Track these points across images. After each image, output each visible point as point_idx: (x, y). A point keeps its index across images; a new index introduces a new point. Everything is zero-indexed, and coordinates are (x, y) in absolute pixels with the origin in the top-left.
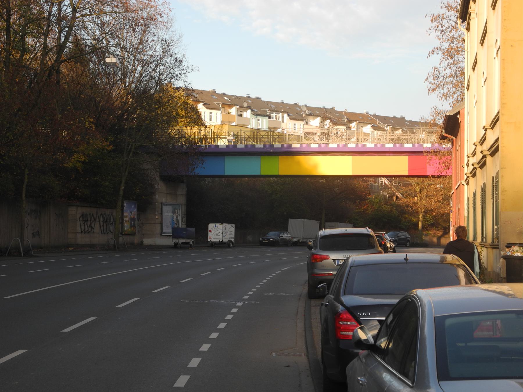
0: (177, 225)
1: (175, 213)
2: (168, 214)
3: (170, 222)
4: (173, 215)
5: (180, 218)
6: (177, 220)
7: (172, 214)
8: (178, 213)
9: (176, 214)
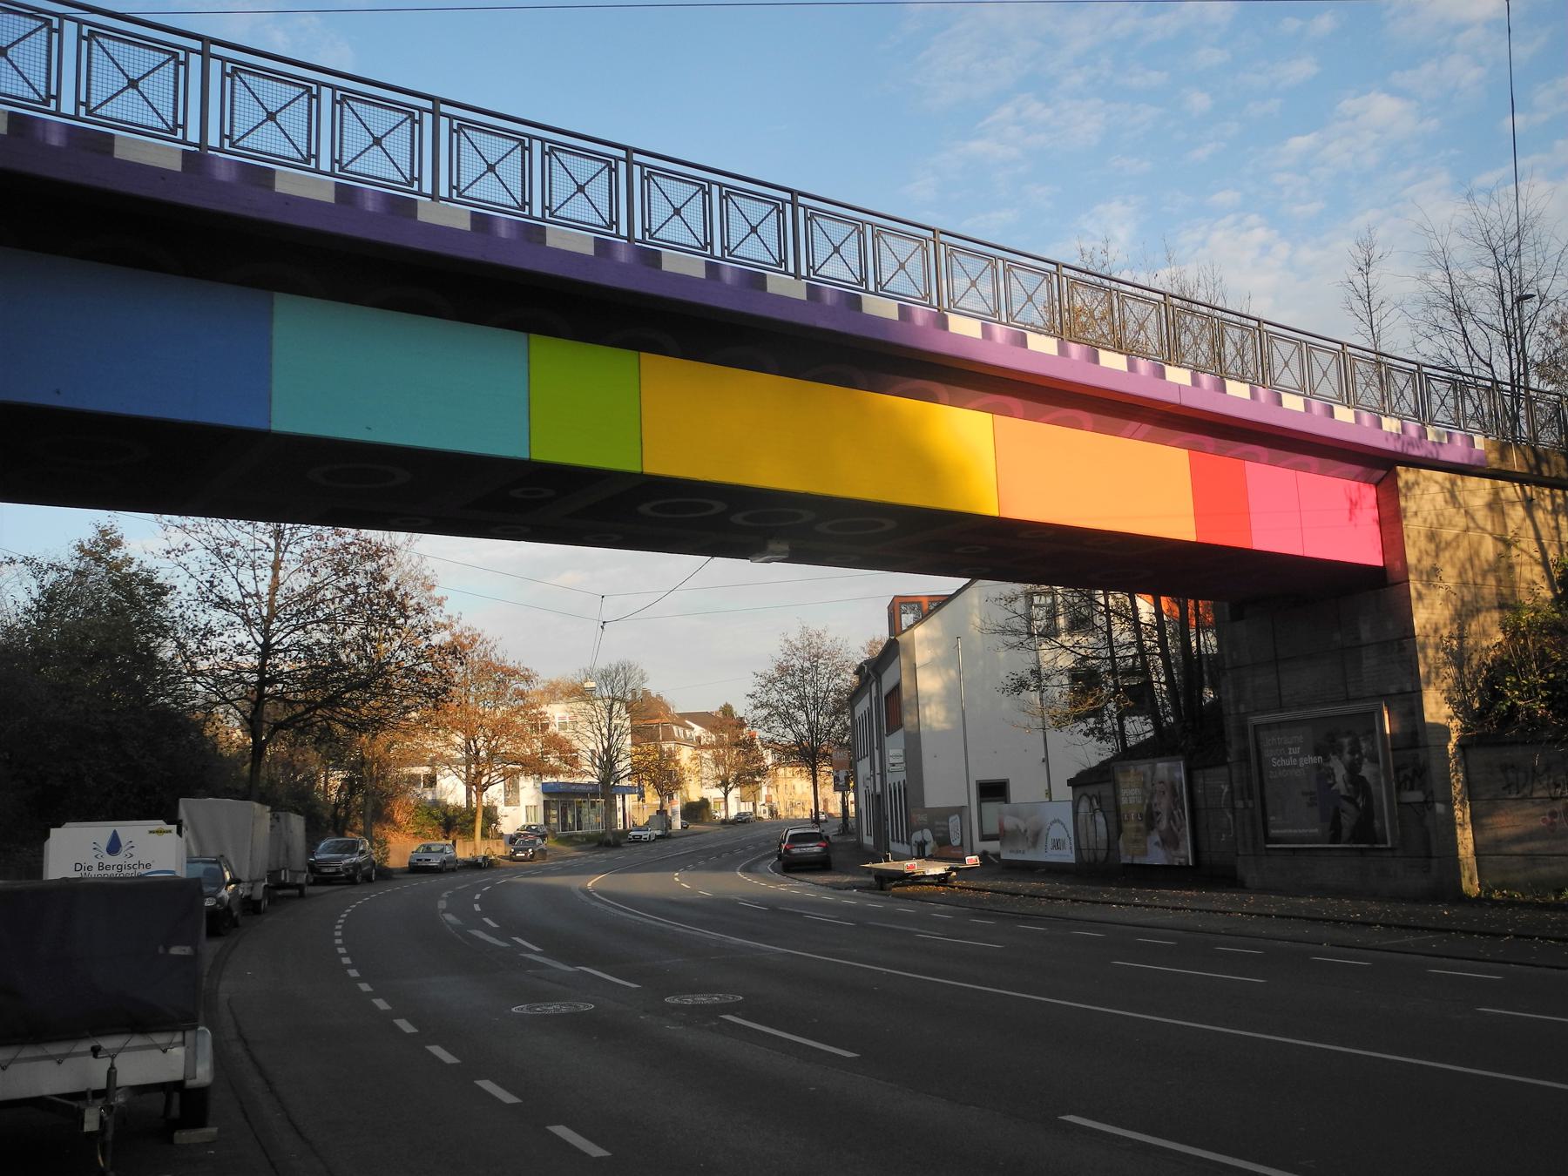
0: (1357, 806)
1: (1338, 751)
2: (1293, 762)
4: (1327, 759)
7: (1312, 760)
8: (1355, 749)
9: (1347, 757)
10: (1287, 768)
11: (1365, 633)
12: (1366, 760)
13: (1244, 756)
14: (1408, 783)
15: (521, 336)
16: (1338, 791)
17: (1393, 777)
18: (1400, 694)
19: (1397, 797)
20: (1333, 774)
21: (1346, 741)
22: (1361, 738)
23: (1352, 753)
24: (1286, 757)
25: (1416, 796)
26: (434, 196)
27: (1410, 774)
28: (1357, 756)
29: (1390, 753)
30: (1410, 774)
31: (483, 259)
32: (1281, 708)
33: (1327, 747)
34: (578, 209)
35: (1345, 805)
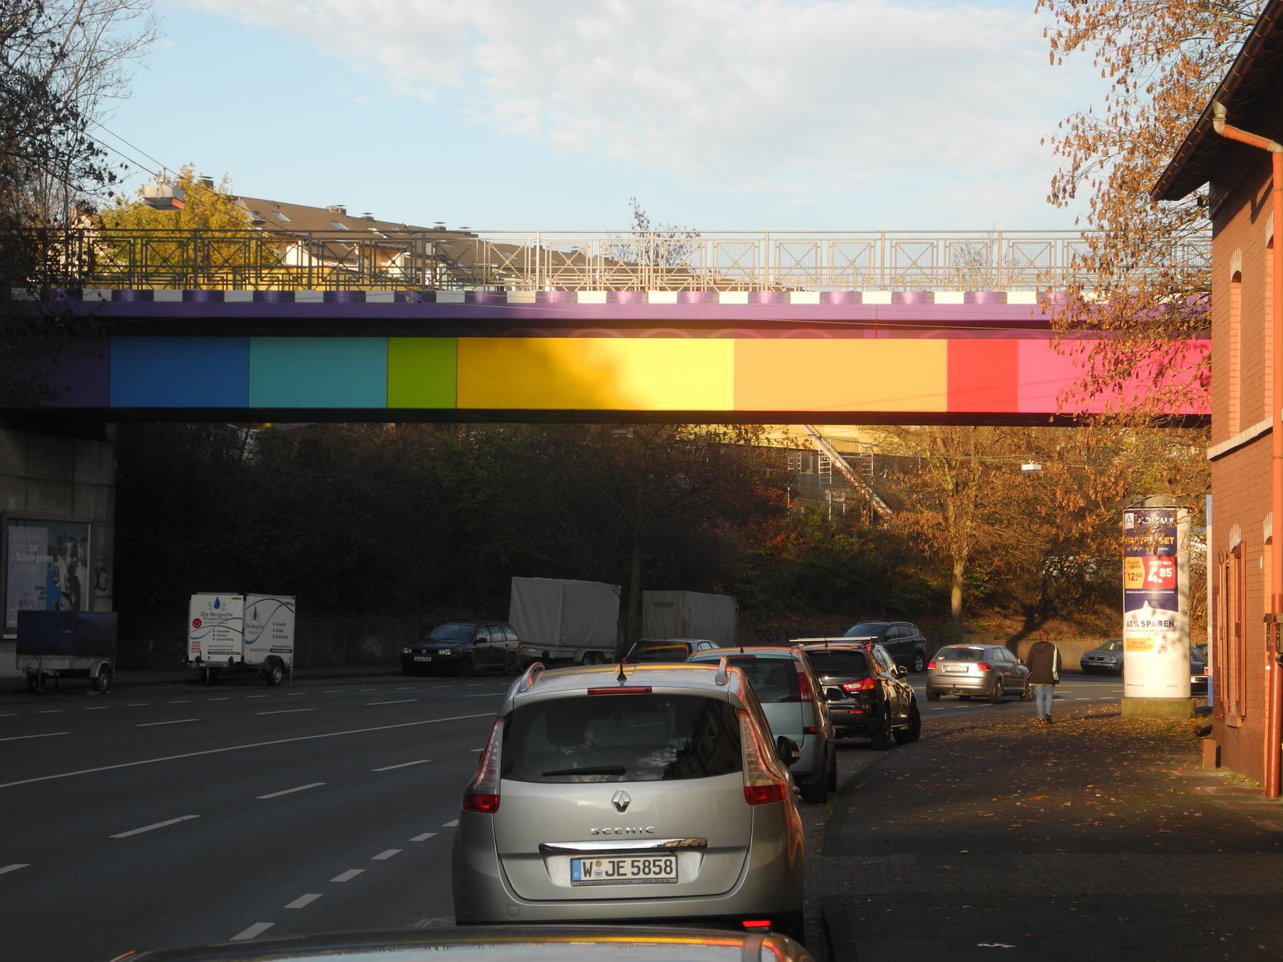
0: (70, 601)
1: (64, 553)
2: (31, 558)
3: (42, 588)
4: (56, 560)
5: (83, 574)
6: (73, 580)
7: (47, 558)
8: (74, 554)
9: (69, 558)
12: (80, 563)
21: (69, 545)
22: (79, 545)
23: (72, 556)
24: (27, 553)
28: (75, 559)
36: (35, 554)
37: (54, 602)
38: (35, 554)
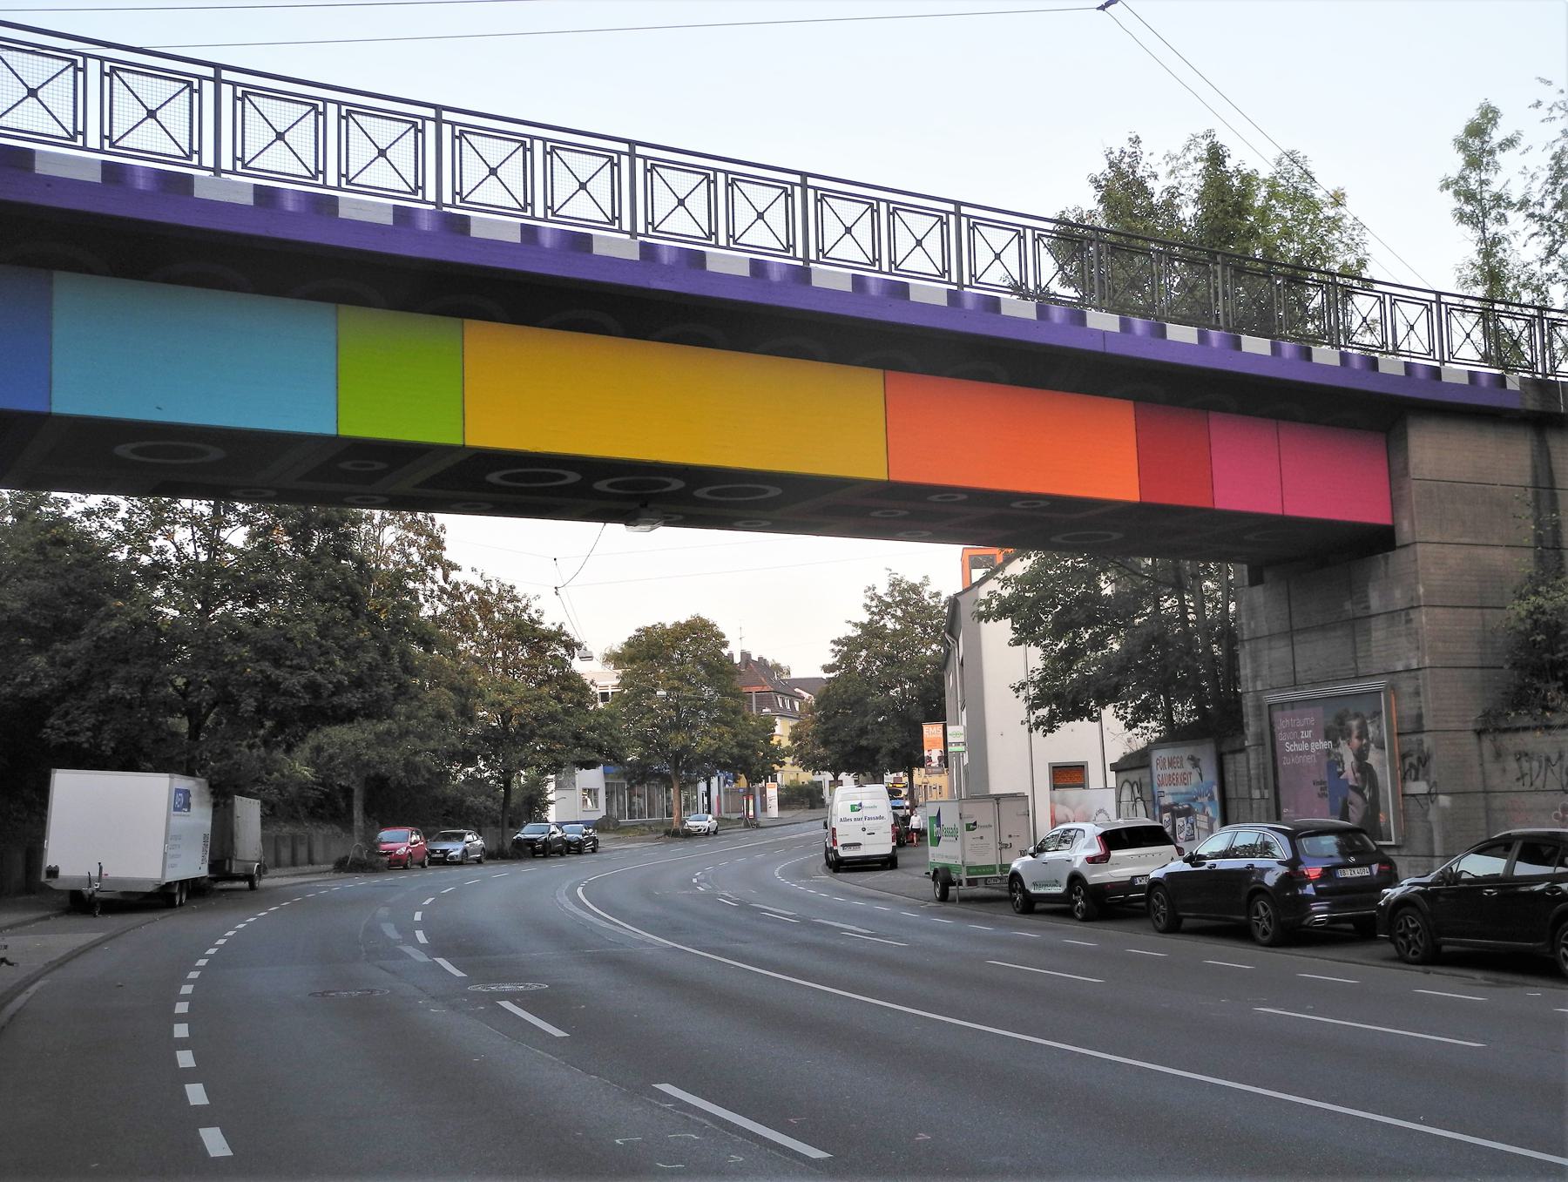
0: (1363, 796)
1: (1346, 734)
2: (1305, 746)
3: (1322, 783)
6: (1364, 769)
7: (1324, 745)
8: (1363, 734)
9: (1355, 742)
10: (1301, 753)
11: (1375, 603)
12: (1372, 745)
13: (1260, 742)
14: (1413, 772)
15: (332, 306)
16: (1346, 780)
17: (1398, 766)
18: (1407, 671)
19: (1402, 787)
20: (1342, 761)
21: (1354, 723)
23: (1360, 737)
24: (1299, 742)
25: (1419, 787)
26: (217, 170)
27: (1415, 762)
28: (1365, 741)
29: (1396, 738)
30: (1415, 762)
31: (268, 235)
32: (1295, 685)
33: (1336, 732)
34: (380, 176)
35: (1354, 796)
36: (1308, 741)
37: (1340, 799)
38: (1308, 741)
